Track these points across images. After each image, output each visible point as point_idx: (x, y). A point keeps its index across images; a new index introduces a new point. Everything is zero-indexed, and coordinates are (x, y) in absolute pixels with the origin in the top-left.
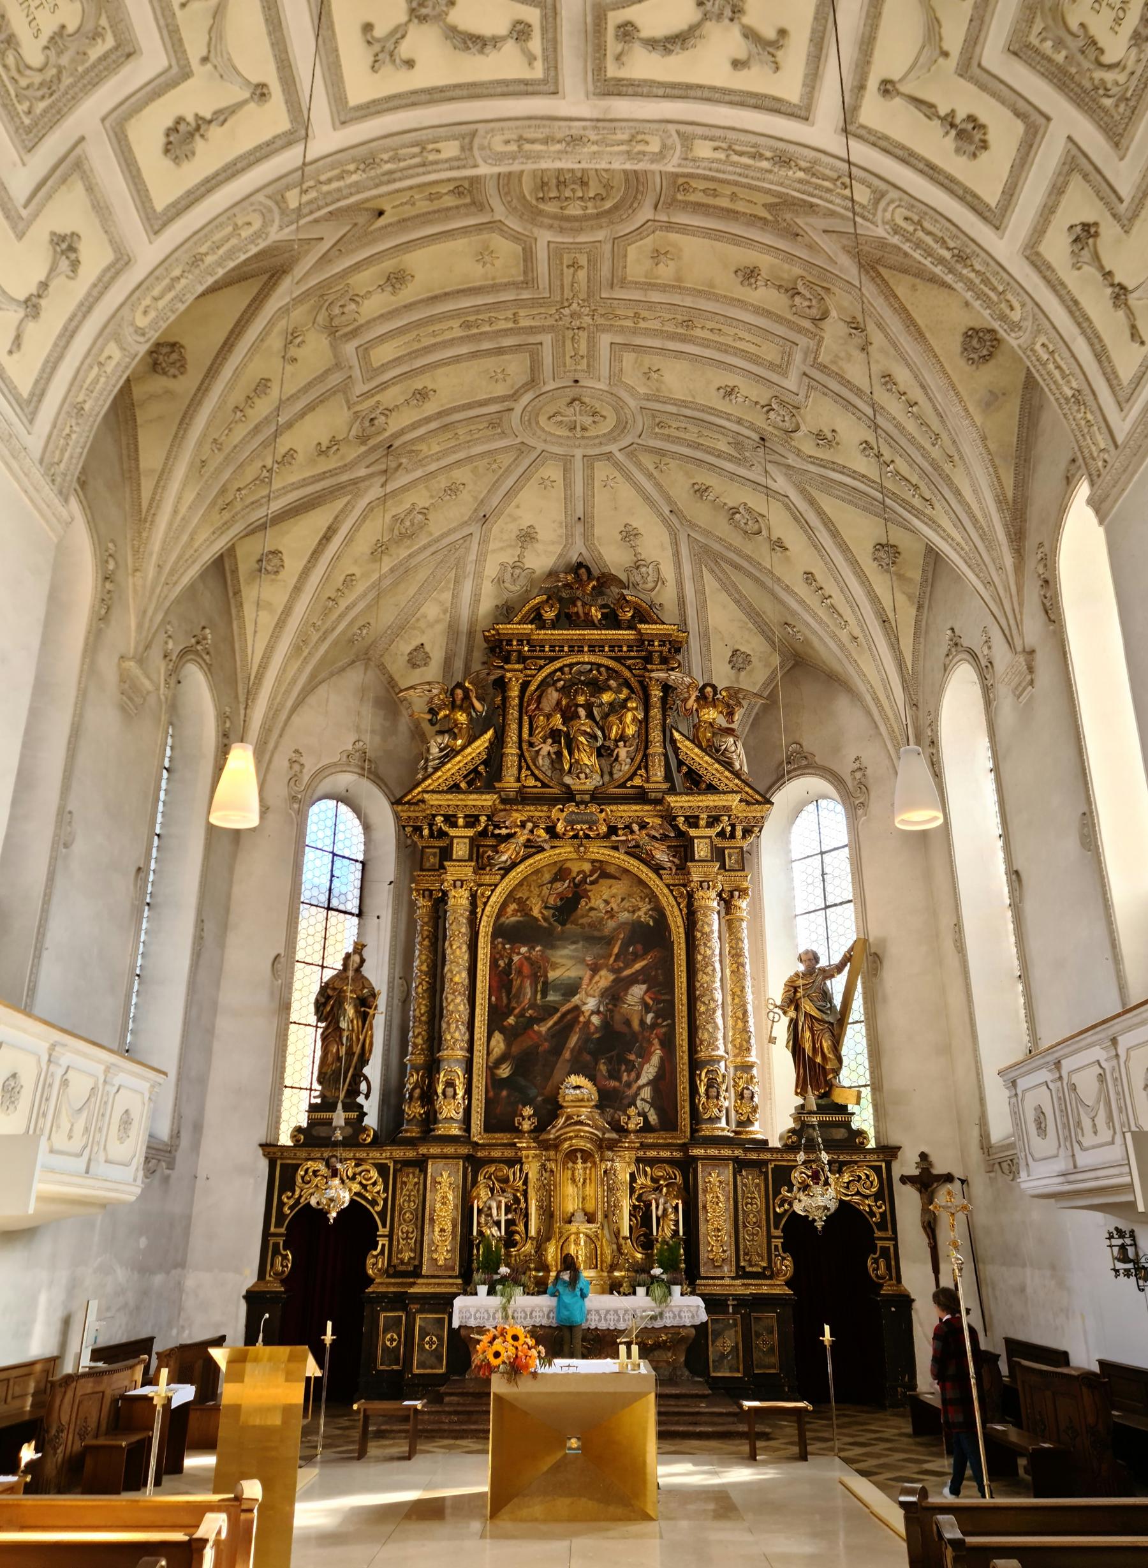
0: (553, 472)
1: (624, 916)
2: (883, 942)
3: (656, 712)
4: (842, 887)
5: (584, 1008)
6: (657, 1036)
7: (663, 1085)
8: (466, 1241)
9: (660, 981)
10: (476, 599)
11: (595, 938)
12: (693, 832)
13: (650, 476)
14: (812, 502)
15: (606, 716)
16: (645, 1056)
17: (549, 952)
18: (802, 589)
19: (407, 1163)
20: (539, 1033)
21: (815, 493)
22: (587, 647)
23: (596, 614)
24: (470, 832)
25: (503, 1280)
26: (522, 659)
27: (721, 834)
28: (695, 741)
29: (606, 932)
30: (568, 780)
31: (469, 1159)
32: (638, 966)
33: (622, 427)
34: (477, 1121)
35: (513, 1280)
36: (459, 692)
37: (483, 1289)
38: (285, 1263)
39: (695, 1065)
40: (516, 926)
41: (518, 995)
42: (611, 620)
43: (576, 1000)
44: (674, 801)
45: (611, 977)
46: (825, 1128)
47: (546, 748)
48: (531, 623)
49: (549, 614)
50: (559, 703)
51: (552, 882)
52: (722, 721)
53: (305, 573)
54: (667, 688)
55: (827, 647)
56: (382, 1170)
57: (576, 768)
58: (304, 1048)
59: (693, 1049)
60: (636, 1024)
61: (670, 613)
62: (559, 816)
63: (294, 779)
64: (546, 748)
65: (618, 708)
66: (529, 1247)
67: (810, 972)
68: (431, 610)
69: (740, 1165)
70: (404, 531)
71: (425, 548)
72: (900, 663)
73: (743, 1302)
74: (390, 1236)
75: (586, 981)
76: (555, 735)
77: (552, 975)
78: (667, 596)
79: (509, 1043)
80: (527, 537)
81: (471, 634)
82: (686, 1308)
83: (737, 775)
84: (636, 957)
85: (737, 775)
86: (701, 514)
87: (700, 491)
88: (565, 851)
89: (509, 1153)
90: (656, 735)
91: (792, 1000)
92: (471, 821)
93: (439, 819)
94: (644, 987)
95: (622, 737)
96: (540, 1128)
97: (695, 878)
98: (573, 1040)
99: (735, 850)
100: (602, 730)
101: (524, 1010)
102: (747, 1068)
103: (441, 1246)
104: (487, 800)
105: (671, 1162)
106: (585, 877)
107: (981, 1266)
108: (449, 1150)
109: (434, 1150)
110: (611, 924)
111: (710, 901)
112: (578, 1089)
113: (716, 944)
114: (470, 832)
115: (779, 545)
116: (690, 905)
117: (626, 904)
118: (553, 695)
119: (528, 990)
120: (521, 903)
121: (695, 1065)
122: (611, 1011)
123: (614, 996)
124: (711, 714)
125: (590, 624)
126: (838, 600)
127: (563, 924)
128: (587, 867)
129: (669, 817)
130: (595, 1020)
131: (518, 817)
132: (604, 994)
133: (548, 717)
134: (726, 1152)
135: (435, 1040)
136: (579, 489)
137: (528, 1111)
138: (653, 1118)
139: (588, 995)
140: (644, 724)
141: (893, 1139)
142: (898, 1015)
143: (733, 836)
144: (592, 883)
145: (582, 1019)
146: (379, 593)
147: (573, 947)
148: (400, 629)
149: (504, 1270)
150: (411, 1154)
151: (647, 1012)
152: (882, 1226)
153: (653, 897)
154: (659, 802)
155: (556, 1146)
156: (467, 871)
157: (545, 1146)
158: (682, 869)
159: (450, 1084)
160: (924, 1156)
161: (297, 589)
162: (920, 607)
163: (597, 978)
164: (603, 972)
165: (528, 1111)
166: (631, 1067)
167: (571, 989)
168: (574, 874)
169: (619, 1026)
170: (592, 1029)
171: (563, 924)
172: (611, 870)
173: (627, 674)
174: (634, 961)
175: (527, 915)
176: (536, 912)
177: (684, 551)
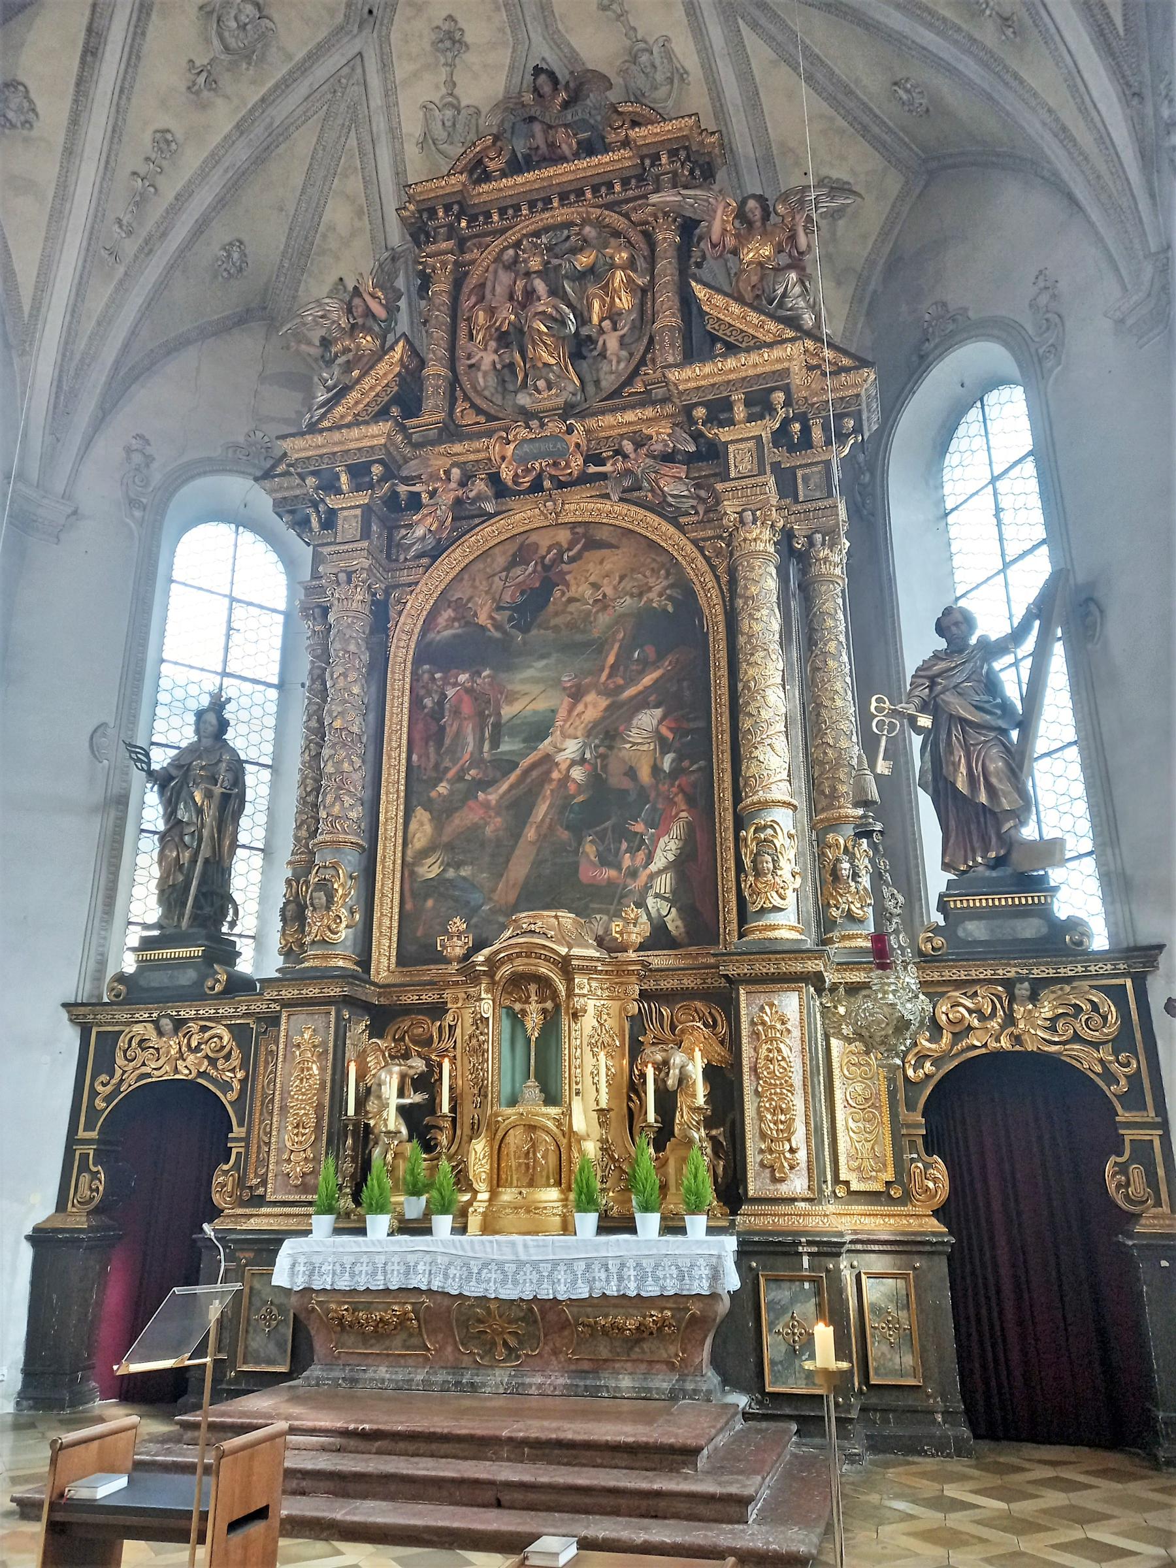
5: (559, 758)
6: (681, 789)
11: (579, 645)
17: (503, 676)
20: (486, 805)
29: (596, 633)
32: (647, 680)
39: (740, 823)
41: (453, 752)
43: (545, 746)
45: (604, 703)
51: (507, 569)
60: (645, 775)
71: (285, 85)
75: (562, 713)
77: (507, 712)
84: (645, 665)
88: (524, 515)
94: (658, 712)
98: (542, 810)
101: (464, 770)
106: (561, 554)
110: (604, 619)
117: (627, 584)
119: (470, 739)
121: (740, 823)
122: (603, 757)
123: (607, 733)
127: (525, 630)
128: (564, 536)
130: (577, 774)
139: (565, 736)
144: (572, 560)
145: (555, 775)
147: (541, 664)
151: (664, 753)
153: (672, 566)
163: (580, 708)
164: (591, 697)
167: (539, 730)
168: (543, 551)
169: (617, 780)
170: (572, 788)
171: (525, 630)
172: (603, 535)
174: (642, 673)
175: (467, 624)
176: (483, 619)
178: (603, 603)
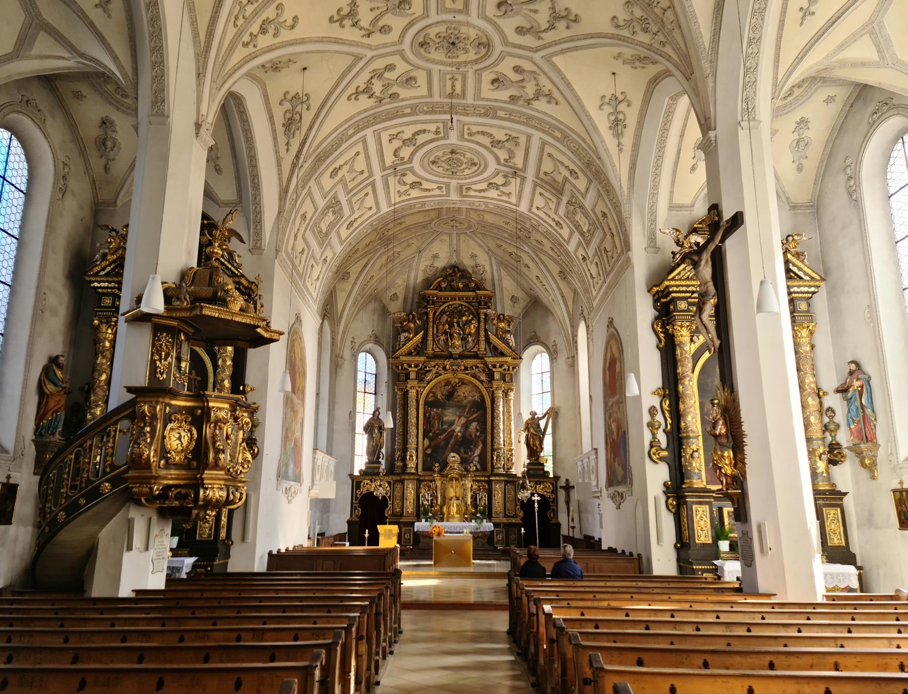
0: (446, 238)
2: (559, 408)
3: (482, 324)
4: (547, 387)
7: (482, 456)
8: (418, 505)
9: (482, 421)
10: (416, 277)
11: (460, 406)
12: (494, 370)
14: (537, 256)
15: (464, 325)
16: (476, 447)
18: (535, 281)
19: (397, 481)
22: (458, 298)
23: (461, 285)
24: (416, 369)
25: (430, 517)
26: (434, 303)
28: (496, 335)
31: (418, 480)
33: (470, 227)
34: (420, 468)
35: (434, 517)
37: (424, 520)
38: (359, 512)
39: (493, 450)
40: (432, 402)
41: (433, 426)
42: (466, 288)
44: (487, 359)
46: (535, 470)
47: (443, 337)
49: (444, 285)
54: (486, 315)
55: (545, 299)
56: (389, 483)
58: (362, 442)
59: (492, 445)
61: (488, 285)
62: (448, 363)
63: (353, 348)
64: (443, 337)
65: (468, 323)
66: (437, 508)
67: (533, 418)
68: (400, 281)
69: (506, 482)
70: (390, 260)
73: (505, 525)
74: (392, 504)
76: (445, 333)
77: (445, 419)
78: (488, 276)
79: (430, 442)
80: (436, 257)
81: (414, 288)
82: (487, 526)
83: (511, 348)
84: (474, 413)
85: (511, 348)
86: (500, 252)
87: (500, 246)
88: (449, 375)
89: (431, 478)
90: (482, 333)
91: (527, 428)
92: (416, 366)
93: (405, 365)
95: (470, 334)
96: (441, 471)
98: (452, 441)
99: (509, 377)
102: (511, 450)
103: (410, 507)
104: (422, 359)
105: (485, 481)
107: (583, 515)
108: (412, 477)
109: (407, 477)
110: (465, 401)
111: (500, 394)
112: (454, 458)
113: (501, 409)
114: (416, 369)
115: (527, 266)
116: (493, 395)
120: (434, 393)
121: (493, 450)
123: (466, 426)
124: (502, 325)
125: (459, 290)
126: (547, 286)
128: (457, 381)
129: (486, 364)
130: (460, 434)
131: (433, 363)
132: (463, 425)
133: (444, 325)
134: (502, 478)
135: (405, 442)
136: (455, 242)
137: (437, 465)
138: (479, 467)
140: (478, 329)
141: (559, 474)
142: (561, 432)
146: (381, 280)
148: (387, 289)
149: (430, 514)
150: (398, 478)
152: (553, 502)
153: (480, 392)
154: (482, 358)
155: (447, 476)
156: (415, 383)
157: (443, 476)
158: (490, 382)
159: (411, 456)
160: (567, 480)
161: (355, 284)
165: (437, 465)
166: (471, 450)
167: (451, 424)
169: (467, 436)
177: (494, 262)
178: (465, 398)
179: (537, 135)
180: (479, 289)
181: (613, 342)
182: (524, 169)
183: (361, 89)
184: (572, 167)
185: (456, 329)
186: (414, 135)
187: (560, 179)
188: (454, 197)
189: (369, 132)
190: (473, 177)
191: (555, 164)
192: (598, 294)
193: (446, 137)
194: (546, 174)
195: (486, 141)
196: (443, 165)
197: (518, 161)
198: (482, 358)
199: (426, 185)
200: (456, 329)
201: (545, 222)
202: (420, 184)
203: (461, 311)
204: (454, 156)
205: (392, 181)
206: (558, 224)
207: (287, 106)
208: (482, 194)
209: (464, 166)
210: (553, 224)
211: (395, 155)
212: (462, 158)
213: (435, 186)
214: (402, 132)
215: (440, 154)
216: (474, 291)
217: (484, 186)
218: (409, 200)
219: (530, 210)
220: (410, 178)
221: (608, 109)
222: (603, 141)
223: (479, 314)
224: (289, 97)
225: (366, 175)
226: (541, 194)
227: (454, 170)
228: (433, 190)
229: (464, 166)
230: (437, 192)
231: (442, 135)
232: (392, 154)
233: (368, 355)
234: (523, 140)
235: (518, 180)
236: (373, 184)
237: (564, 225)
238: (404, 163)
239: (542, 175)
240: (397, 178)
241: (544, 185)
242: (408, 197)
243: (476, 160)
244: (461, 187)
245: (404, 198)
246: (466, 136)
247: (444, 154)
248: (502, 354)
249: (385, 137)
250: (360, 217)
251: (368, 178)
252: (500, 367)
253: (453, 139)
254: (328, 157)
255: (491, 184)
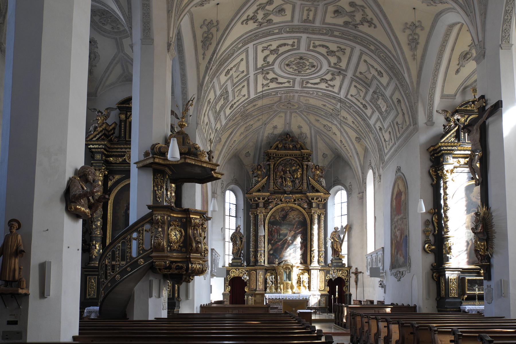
1: (297, 219)
3: (305, 172)
11: (291, 224)
12: (312, 201)
13: (305, 116)
21: (343, 125)
24: (263, 201)
27: (319, 201)
28: (314, 179)
30: (284, 188)
33: (299, 108)
36: (259, 167)
42: (295, 148)
47: (280, 180)
48: (275, 149)
49: (280, 146)
50: (282, 169)
52: (320, 174)
53: (226, 142)
54: (307, 165)
57: (286, 186)
61: (308, 146)
64: (280, 180)
65: (296, 171)
72: (360, 164)
77: (281, 232)
78: (308, 140)
81: (260, 149)
83: (323, 187)
85: (323, 187)
88: (284, 205)
95: (297, 178)
97: (313, 211)
100: (292, 176)
110: (294, 221)
115: (335, 134)
116: (311, 217)
118: (281, 168)
120: (274, 216)
125: (289, 149)
128: (289, 208)
129: (307, 197)
133: (280, 173)
136: (288, 118)
140: (302, 174)
143: (321, 201)
153: (303, 215)
161: (224, 146)
162: (365, 152)
172: (294, 209)
173: (298, 161)
176: (277, 218)
178: (294, 219)
179: (358, 48)
180: (303, 149)
181: (400, 182)
182: (346, 70)
183: (250, 17)
184: (379, 69)
185: (288, 175)
186: (278, 47)
187: (370, 77)
188: (297, 87)
189: (250, 45)
190: (312, 74)
191: (368, 67)
192: (389, 152)
193: (298, 48)
194: (361, 73)
195: (324, 51)
196: (294, 67)
197: (343, 65)
198: (305, 194)
199: (280, 80)
200: (288, 175)
201: (356, 105)
202: (277, 79)
203: (291, 163)
204: (302, 61)
205: (260, 77)
206: (365, 106)
207: (205, 29)
208: (316, 86)
209: (307, 67)
210: (361, 106)
211: (264, 61)
212: (306, 62)
213: (285, 80)
214: (271, 45)
215: (292, 59)
216: (299, 150)
217: (318, 80)
218: (269, 89)
219: (346, 97)
220: (271, 76)
221: (408, 32)
222: (403, 53)
223: (303, 166)
224: (206, 23)
225: (245, 73)
226: (355, 86)
227: (300, 70)
228: (284, 83)
229: (307, 67)
230: (287, 85)
231: (296, 47)
232: (262, 59)
233: (231, 192)
234: (348, 51)
235: (341, 76)
236: (248, 80)
237: (369, 107)
238: (270, 65)
239: (358, 74)
240: (264, 75)
241: (358, 80)
242: (268, 88)
243: (315, 64)
244: (303, 81)
245: (265, 88)
246: (311, 48)
247: (295, 59)
248: (317, 191)
249: (260, 48)
250: (238, 101)
251: (246, 75)
252: (316, 199)
253: (303, 50)
254: (226, 62)
255: (323, 79)
